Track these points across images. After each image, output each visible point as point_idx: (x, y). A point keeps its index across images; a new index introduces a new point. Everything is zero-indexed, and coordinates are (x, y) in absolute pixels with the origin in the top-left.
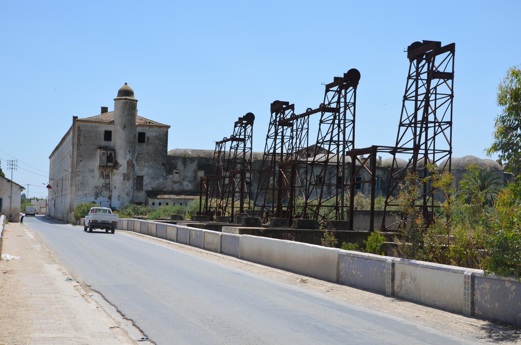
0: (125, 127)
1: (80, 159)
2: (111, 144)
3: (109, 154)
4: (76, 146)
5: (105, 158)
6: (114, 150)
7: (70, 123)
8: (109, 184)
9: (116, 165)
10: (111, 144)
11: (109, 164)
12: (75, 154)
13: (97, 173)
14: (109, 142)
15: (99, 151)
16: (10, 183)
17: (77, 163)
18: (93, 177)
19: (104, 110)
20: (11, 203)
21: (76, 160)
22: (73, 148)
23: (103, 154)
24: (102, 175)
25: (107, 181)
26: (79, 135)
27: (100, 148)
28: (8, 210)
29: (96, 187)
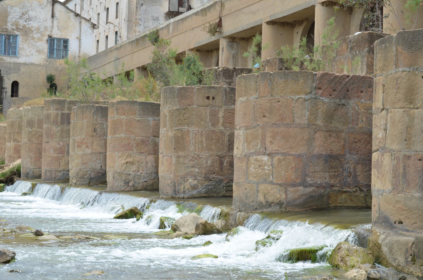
16: (78, 17)
17: (137, 8)
20: (80, 47)
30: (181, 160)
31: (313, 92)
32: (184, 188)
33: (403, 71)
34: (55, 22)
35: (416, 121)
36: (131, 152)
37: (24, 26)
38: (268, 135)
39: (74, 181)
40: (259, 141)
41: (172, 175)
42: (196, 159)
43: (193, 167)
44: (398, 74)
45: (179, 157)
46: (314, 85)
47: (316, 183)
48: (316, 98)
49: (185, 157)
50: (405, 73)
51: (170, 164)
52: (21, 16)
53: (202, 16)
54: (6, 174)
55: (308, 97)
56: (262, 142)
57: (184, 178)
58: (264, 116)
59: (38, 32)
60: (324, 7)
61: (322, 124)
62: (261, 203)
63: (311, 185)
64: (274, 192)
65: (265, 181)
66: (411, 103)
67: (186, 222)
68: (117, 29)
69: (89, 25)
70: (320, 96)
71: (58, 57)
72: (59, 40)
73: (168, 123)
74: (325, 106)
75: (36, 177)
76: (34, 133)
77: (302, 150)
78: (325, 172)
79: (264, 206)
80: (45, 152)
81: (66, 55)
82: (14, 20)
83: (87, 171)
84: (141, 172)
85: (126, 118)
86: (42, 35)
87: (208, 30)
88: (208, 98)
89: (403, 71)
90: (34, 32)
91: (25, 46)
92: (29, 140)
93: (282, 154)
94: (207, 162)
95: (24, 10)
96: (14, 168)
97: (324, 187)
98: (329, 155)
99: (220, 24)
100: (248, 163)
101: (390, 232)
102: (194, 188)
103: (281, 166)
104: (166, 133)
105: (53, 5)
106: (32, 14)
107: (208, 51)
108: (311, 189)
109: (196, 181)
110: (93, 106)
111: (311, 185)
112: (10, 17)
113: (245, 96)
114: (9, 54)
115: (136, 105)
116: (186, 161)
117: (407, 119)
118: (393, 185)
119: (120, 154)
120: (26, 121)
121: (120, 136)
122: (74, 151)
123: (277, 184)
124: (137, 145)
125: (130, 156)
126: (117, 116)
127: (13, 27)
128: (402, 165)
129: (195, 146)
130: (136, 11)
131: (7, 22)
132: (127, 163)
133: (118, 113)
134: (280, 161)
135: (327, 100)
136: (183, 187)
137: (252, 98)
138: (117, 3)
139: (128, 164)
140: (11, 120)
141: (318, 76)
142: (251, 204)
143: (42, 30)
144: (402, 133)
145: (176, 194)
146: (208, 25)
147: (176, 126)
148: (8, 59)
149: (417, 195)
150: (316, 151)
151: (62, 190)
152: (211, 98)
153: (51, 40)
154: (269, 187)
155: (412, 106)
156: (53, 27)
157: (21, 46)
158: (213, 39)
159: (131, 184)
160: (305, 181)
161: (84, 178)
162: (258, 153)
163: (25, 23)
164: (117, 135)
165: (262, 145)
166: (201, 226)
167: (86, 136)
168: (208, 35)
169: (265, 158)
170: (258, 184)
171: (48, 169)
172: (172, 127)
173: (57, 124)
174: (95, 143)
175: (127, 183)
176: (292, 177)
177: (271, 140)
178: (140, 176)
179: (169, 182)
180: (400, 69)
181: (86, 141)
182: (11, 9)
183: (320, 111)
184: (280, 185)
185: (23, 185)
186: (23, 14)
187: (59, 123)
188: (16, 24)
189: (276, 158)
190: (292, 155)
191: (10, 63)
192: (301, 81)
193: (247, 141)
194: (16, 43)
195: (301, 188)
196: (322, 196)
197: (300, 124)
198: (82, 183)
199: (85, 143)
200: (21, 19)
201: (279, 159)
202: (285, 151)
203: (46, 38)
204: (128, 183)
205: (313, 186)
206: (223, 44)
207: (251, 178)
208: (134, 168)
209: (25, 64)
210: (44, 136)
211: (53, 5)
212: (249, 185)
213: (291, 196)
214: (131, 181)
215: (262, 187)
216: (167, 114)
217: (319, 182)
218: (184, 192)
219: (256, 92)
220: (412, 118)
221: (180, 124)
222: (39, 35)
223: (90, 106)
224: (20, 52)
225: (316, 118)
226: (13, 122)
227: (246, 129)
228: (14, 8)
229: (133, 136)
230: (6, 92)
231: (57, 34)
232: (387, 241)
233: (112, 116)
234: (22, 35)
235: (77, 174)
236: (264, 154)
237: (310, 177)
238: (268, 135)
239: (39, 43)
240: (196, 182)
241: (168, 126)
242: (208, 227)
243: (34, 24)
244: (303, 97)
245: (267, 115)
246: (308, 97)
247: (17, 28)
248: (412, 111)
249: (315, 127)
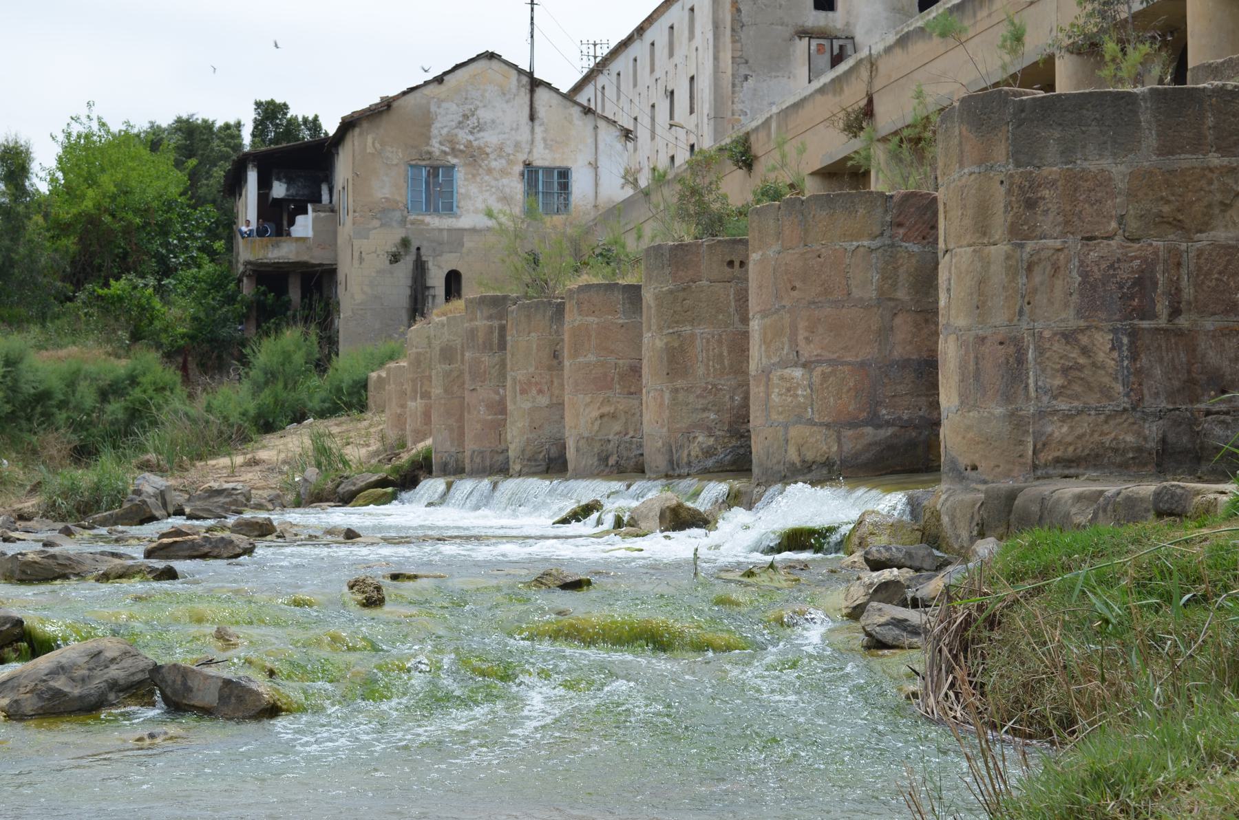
1: (744, 70)
3: (836, 51)
4: (728, 32)
10: (834, 20)
12: (726, 57)
14: (830, 14)
16: (590, 116)
17: (734, 85)
20: (597, 185)
21: (729, 72)
22: (716, 37)
23: (820, 48)
27: (804, 33)
28: (589, 207)
30: (681, 396)
31: (887, 234)
32: (689, 455)
33: (971, 174)
34: (539, 130)
35: (993, 268)
36: (609, 393)
37: (469, 145)
38: (802, 325)
39: (518, 467)
40: (786, 339)
41: (665, 429)
42: (710, 392)
43: (704, 410)
44: (964, 180)
45: (676, 390)
46: (888, 218)
47: (900, 418)
48: (892, 245)
49: (688, 390)
50: (973, 177)
51: (661, 405)
52: (460, 123)
53: (834, 95)
54: (401, 467)
55: (877, 243)
56: (790, 341)
57: (688, 434)
58: (794, 288)
59: (500, 157)
60: (1074, 56)
61: (907, 298)
62: (793, 464)
63: (888, 424)
64: (817, 441)
65: (799, 419)
66: (984, 234)
67: (650, 510)
68: (693, 140)
69: (615, 132)
70: (902, 240)
72: (548, 170)
73: (653, 321)
74: (914, 261)
75: (455, 470)
76: (455, 374)
77: (868, 352)
78: (918, 396)
79: (799, 471)
80: (469, 412)
81: (566, 206)
82: (444, 131)
83: (542, 445)
84: (631, 434)
85: (596, 320)
86: (510, 162)
87: (841, 125)
88: (731, 263)
89: (971, 174)
90: (492, 156)
91: (473, 189)
92: (446, 391)
93: (830, 362)
94: (732, 398)
95: (467, 107)
96: (419, 453)
97: (916, 427)
98: (926, 361)
99: (868, 111)
100: (767, 386)
101: (958, 487)
102: (709, 452)
103: (827, 388)
104: (653, 342)
105: (532, 92)
106: (484, 115)
107: (845, 175)
108: (890, 431)
109: (712, 439)
110: (550, 303)
111: (888, 424)
112: (437, 125)
113: (760, 248)
114: (436, 210)
115: (616, 293)
116: (691, 398)
117: (979, 265)
118: (960, 395)
119: (588, 399)
120: (438, 349)
121: (587, 359)
122: (515, 404)
123: (821, 424)
124: (622, 377)
125: (607, 401)
126: (579, 318)
127: (444, 148)
128: (972, 355)
129: (708, 365)
130: (733, 92)
131: (429, 138)
132: (602, 416)
133: (580, 312)
134: (825, 377)
135: (916, 249)
136: (686, 452)
137: (770, 253)
138: (692, 78)
139: (605, 419)
140: (414, 350)
141: (895, 199)
142: (776, 468)
143: (509, 150)
144: (971, 294)
145: (673, 469)
146: (842, 115)
147: (669, 328)
148: (434, 221)
149: (999, 411)
150: (897, 353)
151: (495, 486)
152: (737, 264)
153: (530, 172)
154: (807, 431)
155: (985, 241)
156: (533, 141)
157: (462, 191)
158: (857, 144)
159: (612, 461)
160: (875, 414)
161: (536, 460)
162: (784, 364)
163: (471, 138)
164: (581, 359)
165: (791, 347)
166: (668, 513)
167: (537, 368)
168: (843, 137)
169: (798, 373)
170: (786, 427)
171: (476, 447)
172: (661, 329)
173: (491, 349)
174: (555, 384)
175: (604, 459)
176: (850, 409)
177: (806, 334)
178: (631, 443)
179: (660, 444)
180: (966, 171)
181: (537, 379)
182: (439, 107)
183: (901, 270)
184: (828, 426)
185: (432, 486)
186: (466, 117)
187: (495, 347)
188: (451, 141)
189: (819, 370)
190: (849, 364)
191: (441, 230)
192: (861, 211)
193: (765, 341)
194: (450, 182)
195: (869, 430)
196: (912, 445)
197: (861, 299)
198: (533, 469)
199: (537, 383)
200: (462, 128)
201: (823, 373)
202: (835, 356)
203: (519, 168)
204: (607, 458)
205: (893, 425)
206: (879, 154)
207: (774, 416)
208: (617, 427)
209: (474, 230)
210: (467, 377)
211: (532, 92)
212: (770, 430)
213: (848, 446)
214: (612, 454)
215: (793, 432)
216: (652, 303)
217: (905, 417)
218: (689, 464)
219: (778, 239)
220: (986, 263)
221: (677, 322)
222: (503, 161)
223: (543, 302)
224: (462, 204)
225: (894, 286)
226: (419, 354)
227: (763, 317)
228: (444, 105)
229: (611, 359)
230: (434, 297)
231: (542, 157)
232: (948, 504)
233: (572, 318)
234: (465, 165)
235: (523, 451)
236: (796, 365)
237: (886, 408)
238: (802, 325)
239: (505, 181)
240: (711, 441)
241: (654, 328)
242: (684, 514)
243: (490, 138)
244: (866, 243)
245: (798, 285)
246: (877, 243)
247: (453, 149)
248: (987, 250)
249: (892, 304)
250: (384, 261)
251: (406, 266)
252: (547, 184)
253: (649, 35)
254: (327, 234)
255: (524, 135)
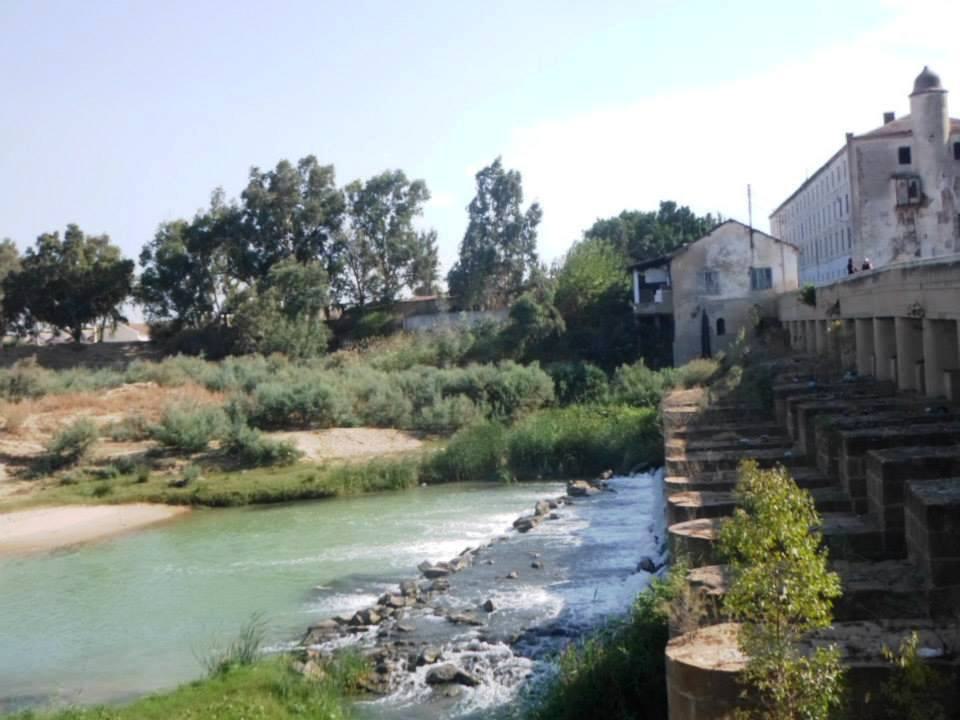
0: (932, 136)
2: (911, 168)
5: (904, 192)
6: (918, 177)
7: (843, 142)
8: (914, 232)
9: (924, 201)
10: (911, 168)
11: (914, 200)
13: (893, 217)
15: (893, 182)
18: (888, 225)
19: (889, 117)
23: (902, 184)
24: (901, 219)
25: (911, 228)
26: (859, 163)
27: (896, 177)
29: (894, 240)
34: (756, 254)
69: (791, 249)
71: (762, 288)
72: (761, 270)
106: (730, 248)
153: (753, 272)
156: (753, 257)
203: (747, 270)
209: (729, 300)
231: (758, 264)
243: (733, 258)
250: (689, 317)
251: (698, 322)
252: (761, 277)
253: (833, 167)
254: (668, 298)
255: (749, 253)
